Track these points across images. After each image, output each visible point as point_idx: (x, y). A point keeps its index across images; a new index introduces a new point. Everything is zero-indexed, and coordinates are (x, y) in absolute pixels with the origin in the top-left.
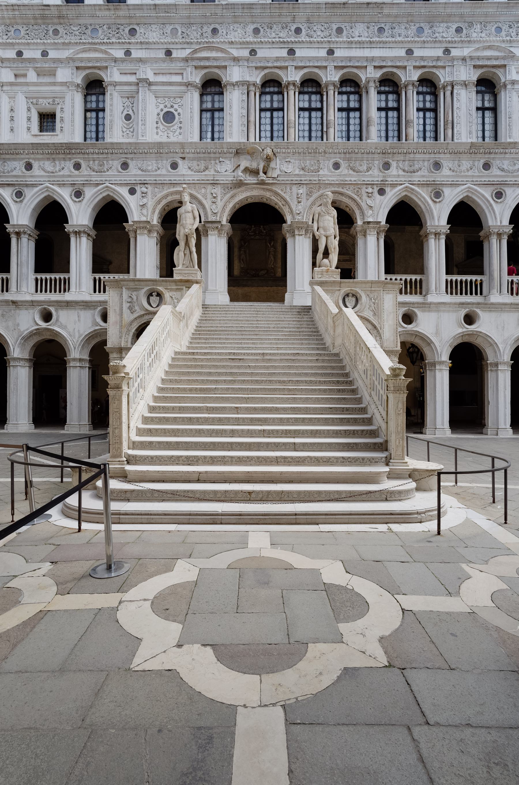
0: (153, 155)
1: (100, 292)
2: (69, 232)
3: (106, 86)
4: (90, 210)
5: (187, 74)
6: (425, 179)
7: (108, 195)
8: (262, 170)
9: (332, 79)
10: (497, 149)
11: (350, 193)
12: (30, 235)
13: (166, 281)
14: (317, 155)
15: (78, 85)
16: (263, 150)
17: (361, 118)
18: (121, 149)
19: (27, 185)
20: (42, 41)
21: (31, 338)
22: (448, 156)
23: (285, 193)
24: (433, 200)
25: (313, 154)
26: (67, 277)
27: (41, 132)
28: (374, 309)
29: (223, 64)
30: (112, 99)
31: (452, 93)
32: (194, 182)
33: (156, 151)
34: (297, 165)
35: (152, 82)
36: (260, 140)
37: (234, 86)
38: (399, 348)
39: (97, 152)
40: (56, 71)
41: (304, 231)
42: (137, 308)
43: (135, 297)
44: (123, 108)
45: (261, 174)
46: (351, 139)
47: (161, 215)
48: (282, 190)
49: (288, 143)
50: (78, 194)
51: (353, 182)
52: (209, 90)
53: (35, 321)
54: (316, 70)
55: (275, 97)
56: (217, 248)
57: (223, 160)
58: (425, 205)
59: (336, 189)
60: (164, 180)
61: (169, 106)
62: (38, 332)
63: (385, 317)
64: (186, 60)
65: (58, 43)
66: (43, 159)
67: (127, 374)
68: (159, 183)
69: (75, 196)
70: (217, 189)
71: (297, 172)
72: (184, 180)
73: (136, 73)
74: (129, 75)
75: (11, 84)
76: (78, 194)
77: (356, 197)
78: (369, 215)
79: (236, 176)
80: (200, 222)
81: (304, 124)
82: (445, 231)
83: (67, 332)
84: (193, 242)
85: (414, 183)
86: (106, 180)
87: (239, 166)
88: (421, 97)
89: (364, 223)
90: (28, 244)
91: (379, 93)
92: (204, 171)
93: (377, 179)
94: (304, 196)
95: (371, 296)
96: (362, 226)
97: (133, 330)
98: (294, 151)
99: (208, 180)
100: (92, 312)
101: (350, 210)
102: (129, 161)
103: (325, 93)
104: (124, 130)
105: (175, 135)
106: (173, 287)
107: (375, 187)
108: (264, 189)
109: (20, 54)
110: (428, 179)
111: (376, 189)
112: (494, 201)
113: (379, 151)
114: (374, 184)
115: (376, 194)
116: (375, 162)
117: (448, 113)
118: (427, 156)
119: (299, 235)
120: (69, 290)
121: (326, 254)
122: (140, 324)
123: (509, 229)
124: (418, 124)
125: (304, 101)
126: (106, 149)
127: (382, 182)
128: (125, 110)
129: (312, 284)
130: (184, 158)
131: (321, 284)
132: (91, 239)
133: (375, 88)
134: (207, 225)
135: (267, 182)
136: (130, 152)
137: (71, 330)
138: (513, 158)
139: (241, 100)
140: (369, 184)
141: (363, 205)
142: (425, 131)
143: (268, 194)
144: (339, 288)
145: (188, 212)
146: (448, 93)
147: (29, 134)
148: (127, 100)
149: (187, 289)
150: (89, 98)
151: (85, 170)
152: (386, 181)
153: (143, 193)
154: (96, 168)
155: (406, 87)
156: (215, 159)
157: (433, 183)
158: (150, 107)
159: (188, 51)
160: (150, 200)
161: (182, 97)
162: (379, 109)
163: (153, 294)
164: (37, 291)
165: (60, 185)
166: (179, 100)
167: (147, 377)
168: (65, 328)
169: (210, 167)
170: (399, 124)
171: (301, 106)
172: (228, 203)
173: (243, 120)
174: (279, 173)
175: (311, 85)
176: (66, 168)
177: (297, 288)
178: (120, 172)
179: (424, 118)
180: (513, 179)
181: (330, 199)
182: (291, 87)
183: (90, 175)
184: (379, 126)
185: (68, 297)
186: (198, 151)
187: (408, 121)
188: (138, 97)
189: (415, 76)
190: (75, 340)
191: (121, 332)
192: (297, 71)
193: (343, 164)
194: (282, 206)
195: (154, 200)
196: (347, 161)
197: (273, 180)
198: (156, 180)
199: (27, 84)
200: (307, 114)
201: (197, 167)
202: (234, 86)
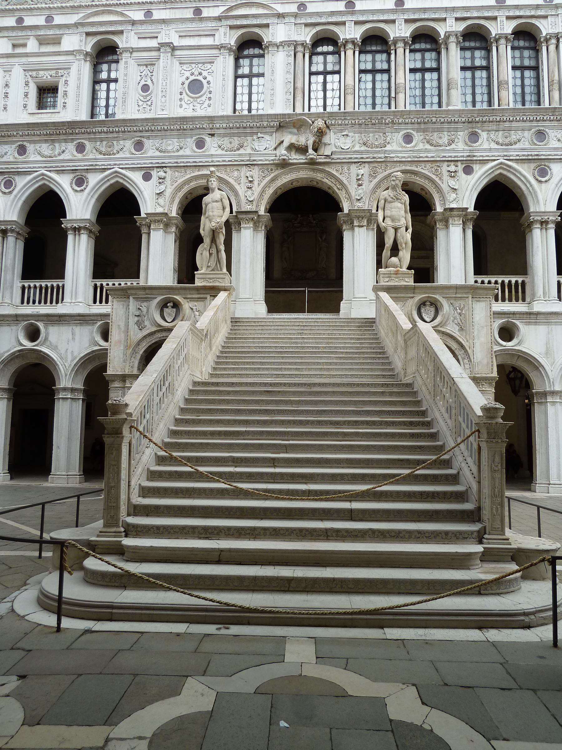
0: (175, 133)
1: (101, 302)
3: (121, 53)
4: (93, 200)
5: (220, 35)
6: (526, 153)
7: (117, 182)
9: (402, 35)
12: (18, 233)
13: (185, 289)
14: (383, 127)
15: (87, 53)
16: (313, 123)
17: (439, 80)
18: (136, 126)
19: (19, 173)
20: (47, 6)
21: (12, 362)
22: (556, 124)
23: (341, 174)
24: (537, 180)
26: (61, 285)
27: (39, 109)
28: (460, 322)
33: (178, 127)
34: (357, 138)
35: (177, 46)
36: (309, 110)
37: (278, 47)
38: (495, 374)
40: (61, 38)
41: (366, 221)
42: (147, 323)
43: (144, 309)
44: (139, 78)
45: (311, 151)
46: (426, 106)
49: (345, 113)
50: (80, 182)
51: (430, 159)
52: (246, 52)
53: (19, 341)
54: (382, 25)
55: (330, 58)
57: (262, 136)
58: (526, 185)
59: (408, 168)
60: (187, 162)
61: (196, 73)
62: (22, 354)
63: (476, 333)
64: (219, 19)
65: (67, 7)
68: (181, 166)
70: (254, 171)
71: (357, 148)
72: (212, 161)
73: (157, 37)
74: (148, 40)
75: (8, 56)
76: (80, 182)
77: (434, 177)
78: (452, 199)
79: (278, 155)
80: (231, 212)
81: (366, 89)
82: (554, 218)
83: (58, 353)
84: (221, 239)
85: (511, 158)
86: (115, 165)
87: (282, 142)
88: (517, 53)
89: (445, 210)
90: (16, 244)
91: (462, 49)
92: (238, 149)
94: (366, 177)
95: (457, 304)
96: (443, 213)
97: (141, 353)
100: (90, 327)
101: (426, 193)
102: (145, 140)
103: (393, 52)
104: (141, 103)
105: (202, 107)
106: (194, 296)
107: (459, 164)
108: (313, 170)
109: (20, 20)
110: (529, 153)
111: (460, 167)
113: (463, 120)
114: (457, 161)
115: (461, 173)
116: (459, 133)
117: (553, 72)
118: (528, 124)
120: (63, 299)
121: (395, 250)
122: (150, 344)
124: (515, 86)
125: (366, 62)
126: (117, 126)
127: (469, 158)
129: (376, 289)
130: (213, 135)
132: (93, 236)
133: (457, 44)
134: (240, 216)
135: (317, 161)
136: (147, 129)
137: (63, 352)
141: (444, 187)
142: (523, 94)
143: (319, 176)
144: (412, 295)
145: (217, 201)
146: (552, 48)
147: (25, 112)
148: (145, 67)
149: (212, 298)
151: (91, 153)
152: (474, 156)
154: (103, 150)
155: (497, 41)
156: (252, 134)
157: (536, 157)
158: (172, 76)
159: (222, 9)
160: (169, 186)
161: (213, 63)
162: (463, 69)
163: (168, 305)
164: (22, 302)
165: (58, 172)
166: (209, 66)
168: (55, 348)
169: (245, 144)
170: (489, 86)
171: (363, 67)
174: (334, 149)
175: (375, 41)
176: (67, 151)
178: (133, 154)
179: (523, 78)
181: (400, 181)
182: (350, 46)
183: (95, 159)
184: (463, 89)
186: (231, 125)
189: (509, 28)
190: (66, 364)
191: (125, 354)
192: (358, 27)
193: (417, 137)
197: (325, 158)
198: (177, 163)
199: (26, 55)
200: (369, 77)
202: (278, 47)
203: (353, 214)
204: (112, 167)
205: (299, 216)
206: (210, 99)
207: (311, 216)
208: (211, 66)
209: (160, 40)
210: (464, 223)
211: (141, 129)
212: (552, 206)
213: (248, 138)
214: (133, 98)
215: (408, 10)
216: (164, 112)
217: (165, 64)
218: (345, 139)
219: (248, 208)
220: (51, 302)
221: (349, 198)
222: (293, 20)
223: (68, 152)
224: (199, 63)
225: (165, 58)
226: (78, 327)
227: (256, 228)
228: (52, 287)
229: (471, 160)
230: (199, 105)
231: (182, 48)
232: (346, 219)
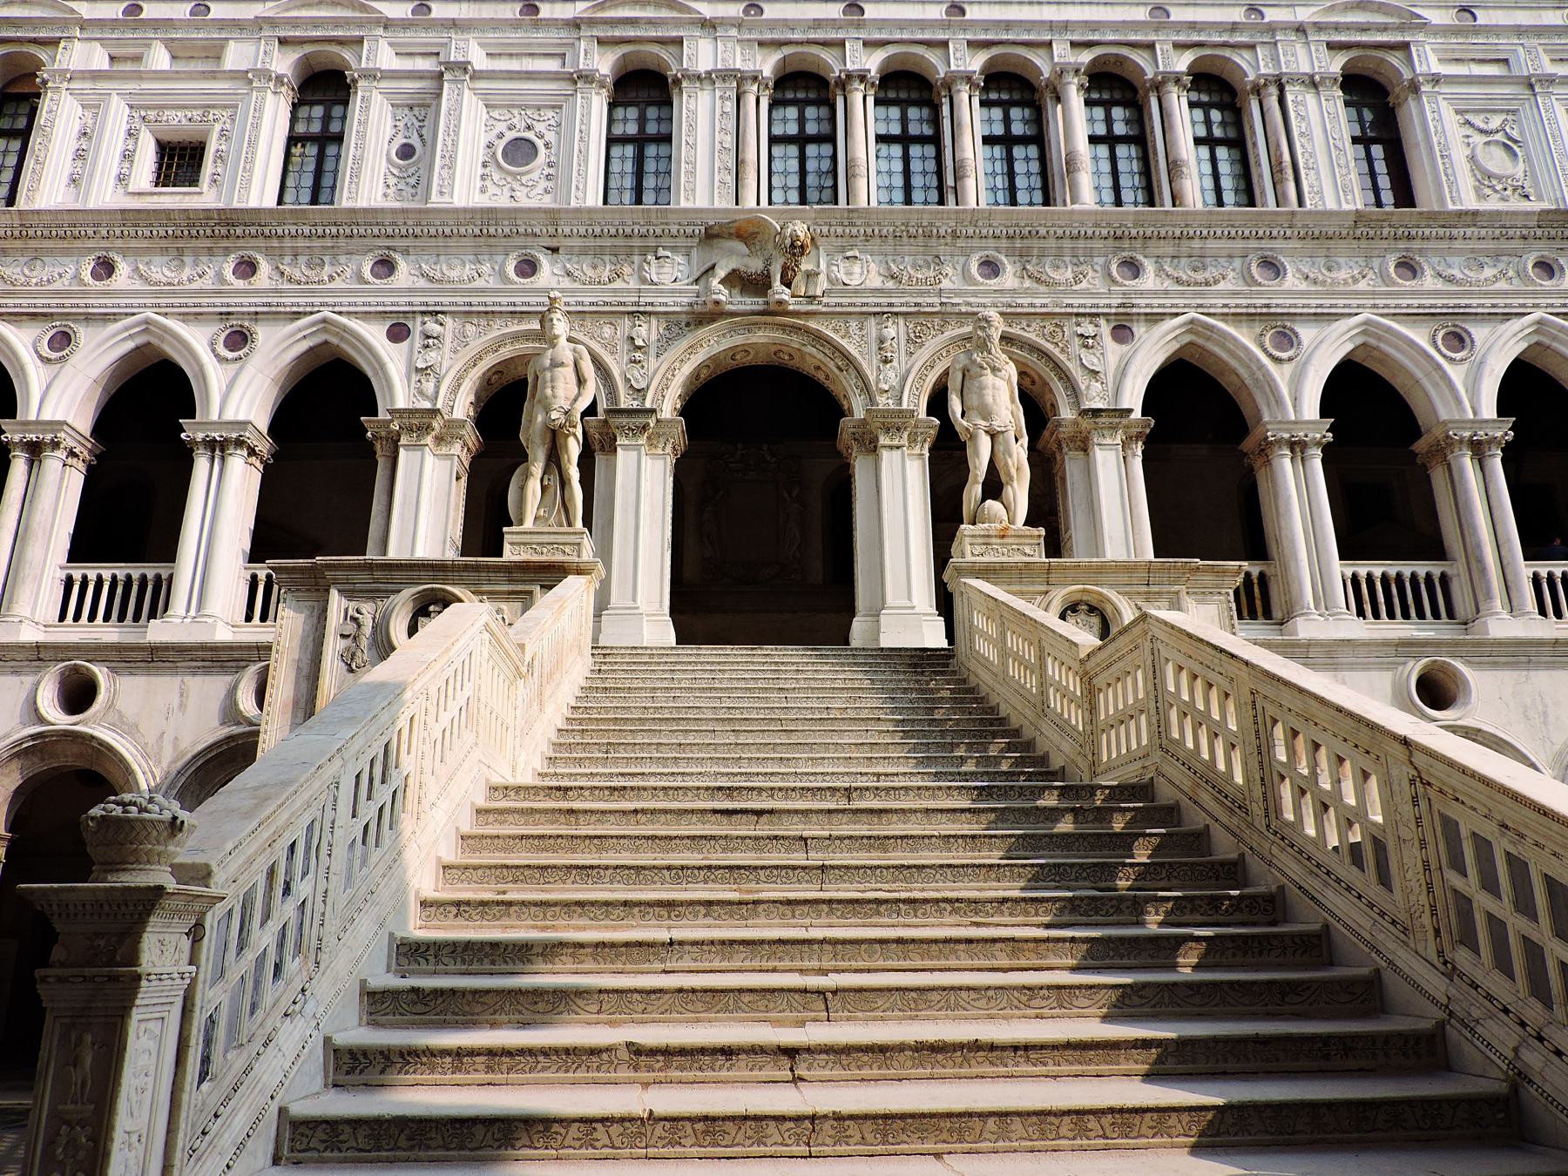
2: (194, 441)
3: (355, 81)
6: (1244, 302)
8: (778, 277)
10: (1429, 226)
11: (1032, 336)
14: (933, 242)
19: (88, 318)
22: (1298, 244)
24: (1270, 356)
25: (921, 239)
29: (674, 34)
30: (366, 109)
31: (1282, 101)
33: (477, 231)
39: (307, 232)
40: (223, 47)
45: (777, 284)
48: (836, 331)
50: (239, 339)
56: (645, 484)
62: (41, 746)
64: (575, 24)
66: (148, 251)
67: (203, 874)
69: (226, 346)
71: (876, 282)
77: (1050, 347)
85: (1212, 310)
87: (713, 267)
98: (869, 231)
99: (624, 304)
100: (229, 678)
101: (1033, 382)
102: (397, 257)
103: (945, 101)
104: (392, 181)
106: (497, 588)
111: (1105, 328)
112: (1444, 356)
113: (1104, 232)
114: (1097, 315)
117: (1278, 146)
119: (891, 447)
120: (166, 610)
123: (1504, 431)
127: (1121, 310)
128: (400, 135)
130: (555, 250)
136: (404, 232)
137: (151, 739)
138: (1473, 251)
139: (718, 111)
140: (1083, 315)
143: (795, 341)
148: (406, 111)
150: (303, 112)
154: (297, 274)
161: (560, 107)
165: (185, 317)
166: (550, 114)
167: (339, 897)
168: (130, 729)
173: (725, 157)
177: (890, 600)
180: (1488, 302)
183: (276, 291)
185: (158, 632)
187: (1175, 162)
188: (439, 106)
200: (897, 150)
201: (590, 272)
207: (765, 447)
209: (442, 58)
211: (390, 231)
212: (1311, 407)
213: (636, 259)
215: (974, 23)
216: (447, 199)
219: (635, 404)
220: (137, 618)
221: (866, 387)
222: (734, 32)
223: (213, 274)
224: (527, 107)
226: (199, 679)
228: (143, 580)
230: (526, 190)
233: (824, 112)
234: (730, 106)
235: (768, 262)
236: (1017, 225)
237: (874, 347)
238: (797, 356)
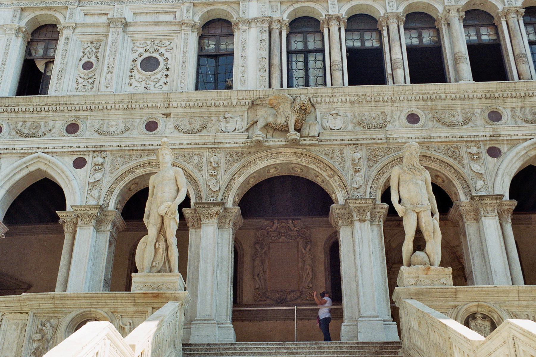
0: (121, 112)
5: (182, 12)
7: (39, 170)
8: (293, 127)
9: (395, 10)
11: (440, 156)
14: (381, 104)
18: (71, 104)
23: (332, 158)
30: (67, 44)
32: (181, 147)
33: (125, 107)
35: (130, 22)
39: (31, 110)
41: (369, 214)
44: (82, 54)
47: (123, 198)
48: (326, 154)
51: (443, 140)
52: (212, 32)
60: (134, 146)
61: (152, 50)
70: (219, 156)
77: (451, 161)
86: (38, 148)
87: (256, 122)
92: (200, 131)
93: (484, 134)
98: (344, 99)
101: (443, 181)
104: (80, 81)
105: (157, 85)
106: (128, 309)
111: (484, 149)
116: (476, 110)
119: (362, 221)
121: (419, 244)
126: (47, 105)
127: (494, 138)
128: (86, 57)
130: (167, 115)
131: (419, 295)
135: (301, 143)
141: (466, 172)
143: (303, 162)
148: (89, 44)
152: (500, 135)
153: (96, 165)
160: (108, 174)
169: (209, 125)
172: (236, 176)
188: (107, 40)
194: (328, 178)
195: (113, 175)
196: (429, 112)
198: (120, 146)
202: (249, 23)
203: (352, 205)
204: (34, 151)
205: (276, 221)
206: (167, 76)
207: (290, 222)
208: (169, 43)
209: (110, 16)
210: (500, 216)
214: (72, 74)
216: (109, 90)
217: (114, 39)
218: (334, 118)
225: (115, 34)
227: (221, 225)
229: (497, 140)
230: (153, 84)
231: (136, 24)
232: (342, 212)
233: (318, 37)
234: (266, 36)
235: (287, 118)
236: (428, 93)
237: (349, 163)
238: (305, 170)
